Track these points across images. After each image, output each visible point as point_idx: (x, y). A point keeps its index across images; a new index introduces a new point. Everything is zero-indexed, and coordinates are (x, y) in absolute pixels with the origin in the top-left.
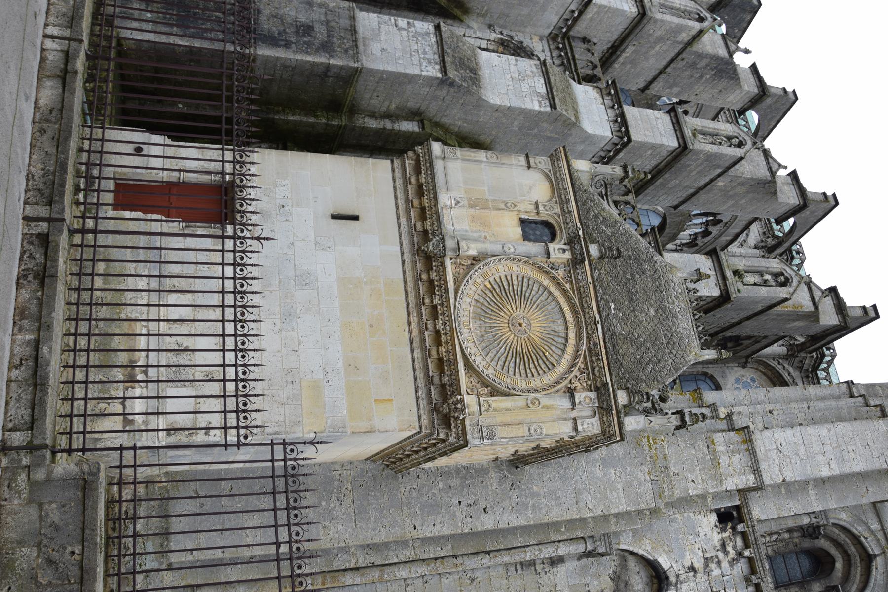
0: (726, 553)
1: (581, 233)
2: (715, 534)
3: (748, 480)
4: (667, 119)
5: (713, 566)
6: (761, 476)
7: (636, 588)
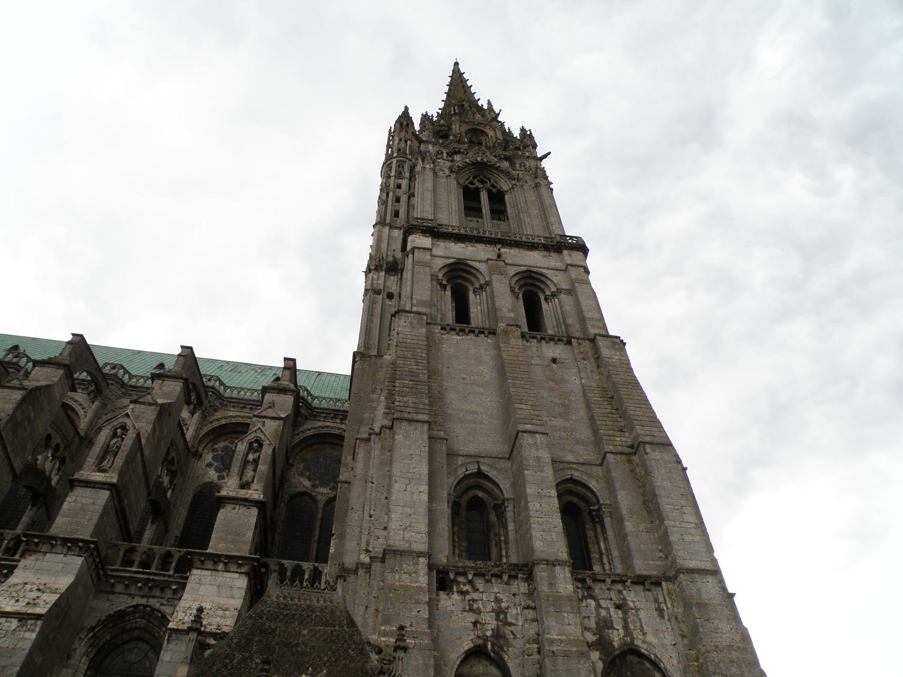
0: (467, 593)
4: (79, 491)
5: (475, 606)
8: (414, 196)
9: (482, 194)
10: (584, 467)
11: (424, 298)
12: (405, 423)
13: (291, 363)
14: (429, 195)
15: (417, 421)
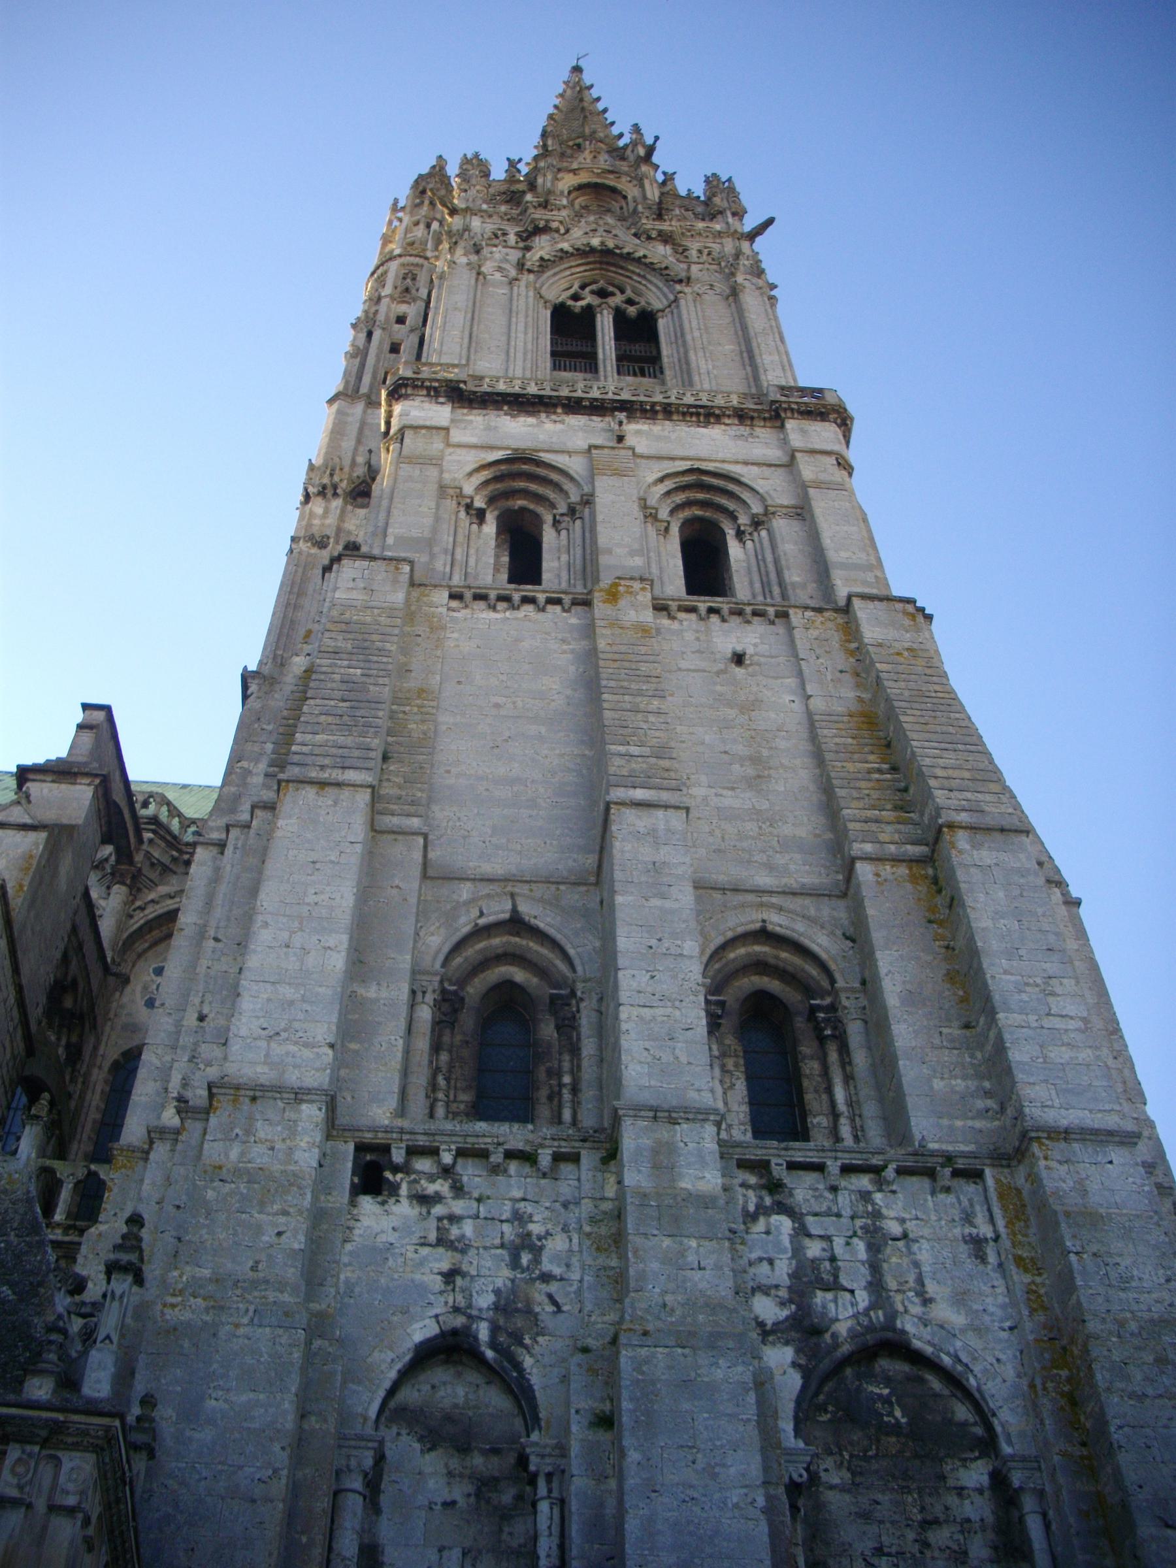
0: (437, 1198)
3: (310, 1116)
5: (455, 1232)
6: (309, 1091)
7: (461, 1401)
10: (799, 901)
11: (415, 533)
12: (310, 792)
13: (100, 716)
14: (459, 320)
15: (338, 785)
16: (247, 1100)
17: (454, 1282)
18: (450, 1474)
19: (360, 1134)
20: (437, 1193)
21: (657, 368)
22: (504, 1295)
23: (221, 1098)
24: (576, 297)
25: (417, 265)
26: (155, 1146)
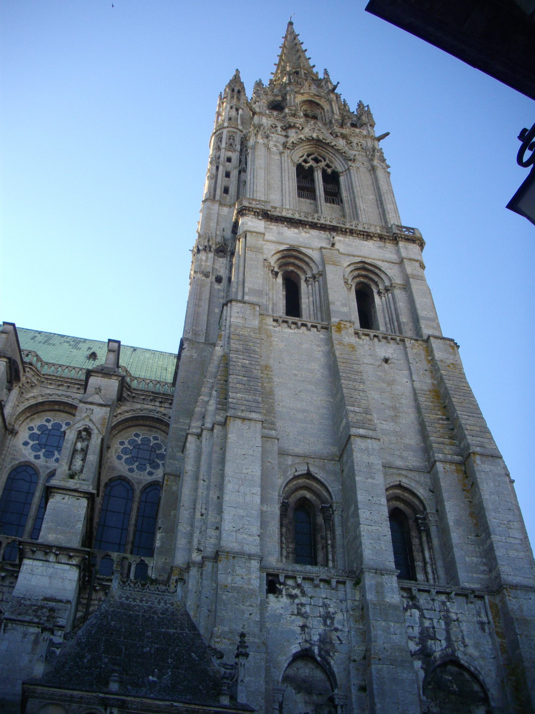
1: (101, 695)
2: (281, 600)
5: (303, 610)
6: (254, 555)
7: (307, 674)
8: (244, 171)
9: (316, 174)
10: (413, 473)
12: (239, 422)
13: (116, 345)
15: (250, 420)
16: (231, 558)
17: (304, 630)
18: (306, 702)
19: (268, 570)
20: (296, 594)
21: (339, 200)
22: (322, 636)
23: (222, 556)
24: (305, 161)
25: (235, 132)
26: (191, 569)
